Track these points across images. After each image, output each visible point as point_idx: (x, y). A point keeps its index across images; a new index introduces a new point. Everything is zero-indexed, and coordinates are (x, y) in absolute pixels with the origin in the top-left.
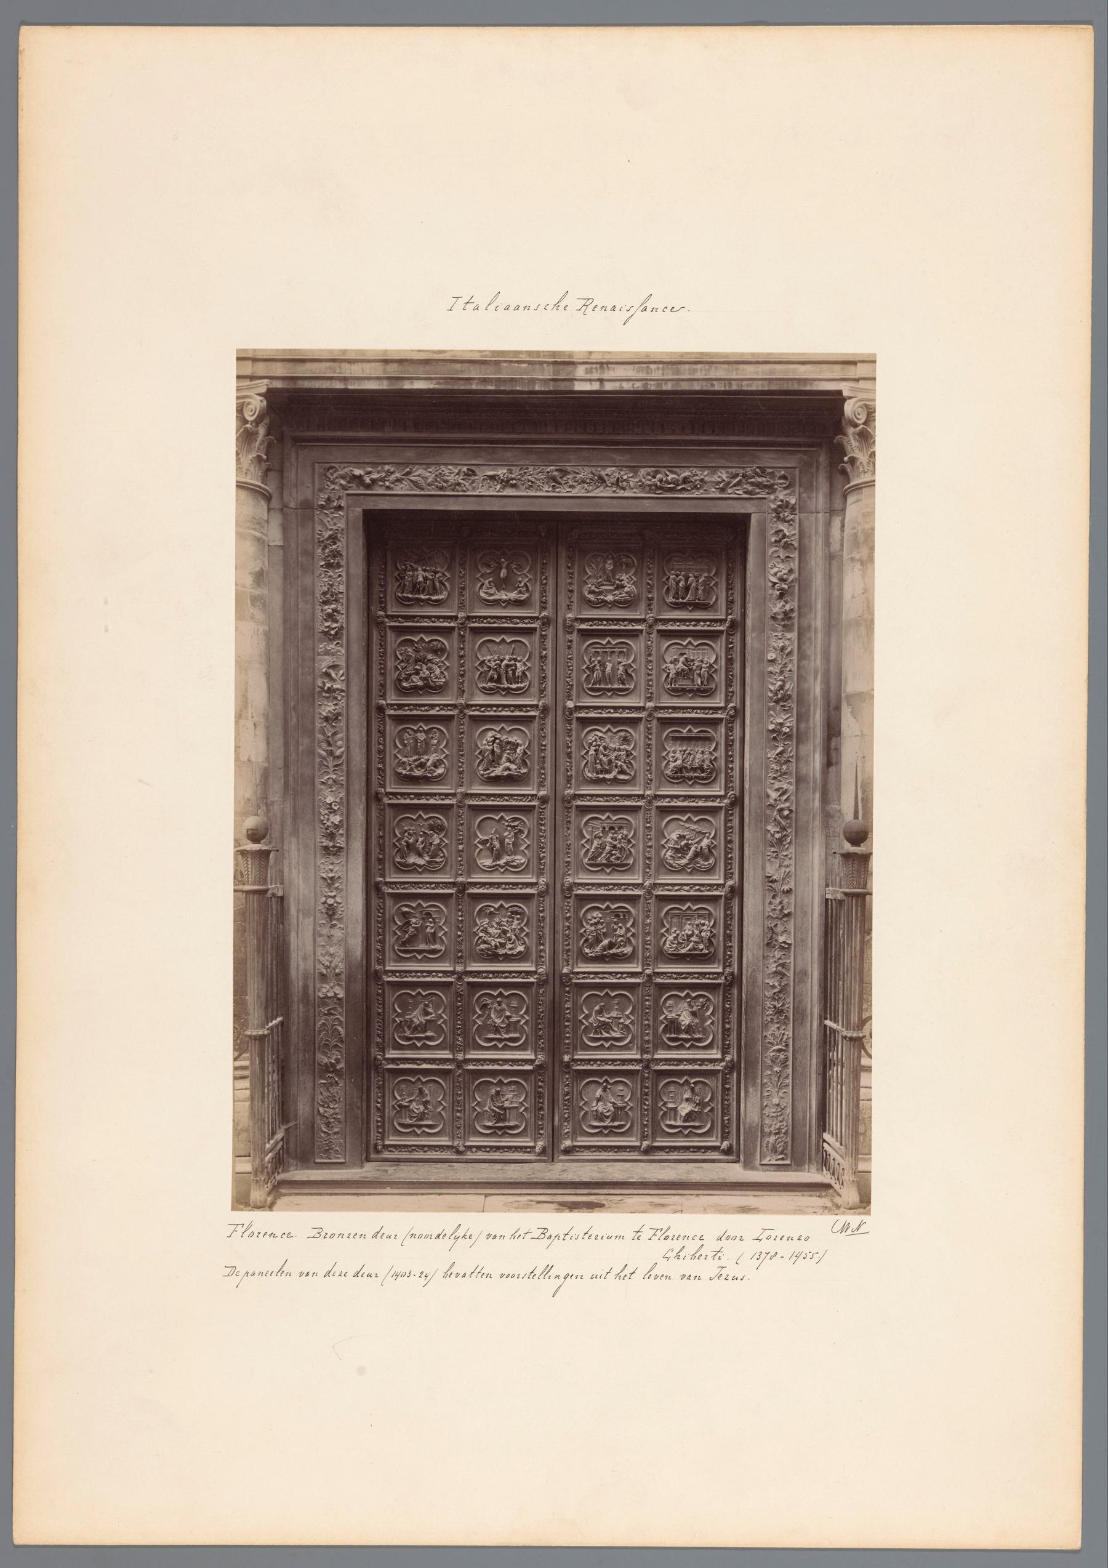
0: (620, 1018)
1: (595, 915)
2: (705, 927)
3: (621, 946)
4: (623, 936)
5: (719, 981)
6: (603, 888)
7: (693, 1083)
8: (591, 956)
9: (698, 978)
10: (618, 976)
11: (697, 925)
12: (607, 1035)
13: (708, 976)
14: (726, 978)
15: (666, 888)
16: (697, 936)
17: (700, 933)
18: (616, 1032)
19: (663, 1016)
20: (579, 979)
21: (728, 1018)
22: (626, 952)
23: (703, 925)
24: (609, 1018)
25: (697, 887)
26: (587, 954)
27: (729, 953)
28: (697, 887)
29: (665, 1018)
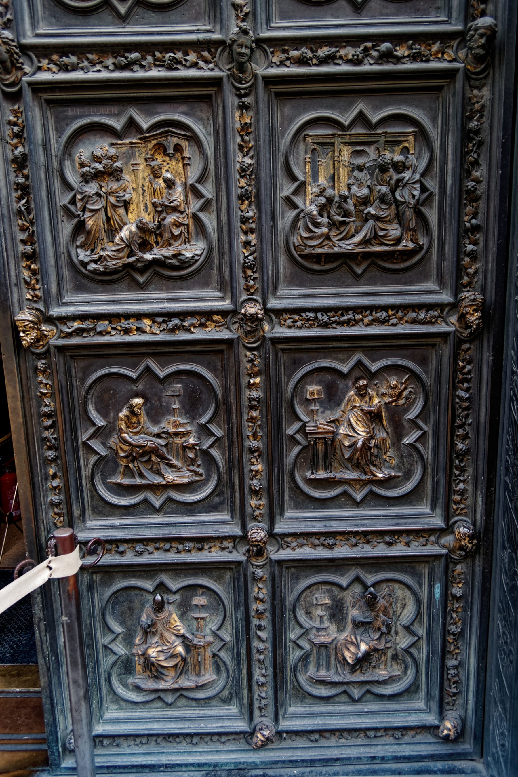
0: (187, 434)
1: (99, 153)
2: (407, 175)
3: (176, 238)
4: (175, 209)
5: (441, 328)
6: (110, 62)
7: (373, 585)
8: (95, 272)
9: (383, 322)
10: (171, 325)
11: (383, 169)
12: (157, 480)
13: (412, 315)
14: (462, 317)
15: (294, 53)
16: (383, 199)
17: (393, 191)
18: (179, 469)
19: (297, 426)
20: (69, 335)
21: (462, 426)
22: (188, 254)
23: (399, 167)
24: (158, 436)
25: (385, 46)
26: (85, 265)
27: (470, 247)
28: (385, 46)
29: (302, 430)
